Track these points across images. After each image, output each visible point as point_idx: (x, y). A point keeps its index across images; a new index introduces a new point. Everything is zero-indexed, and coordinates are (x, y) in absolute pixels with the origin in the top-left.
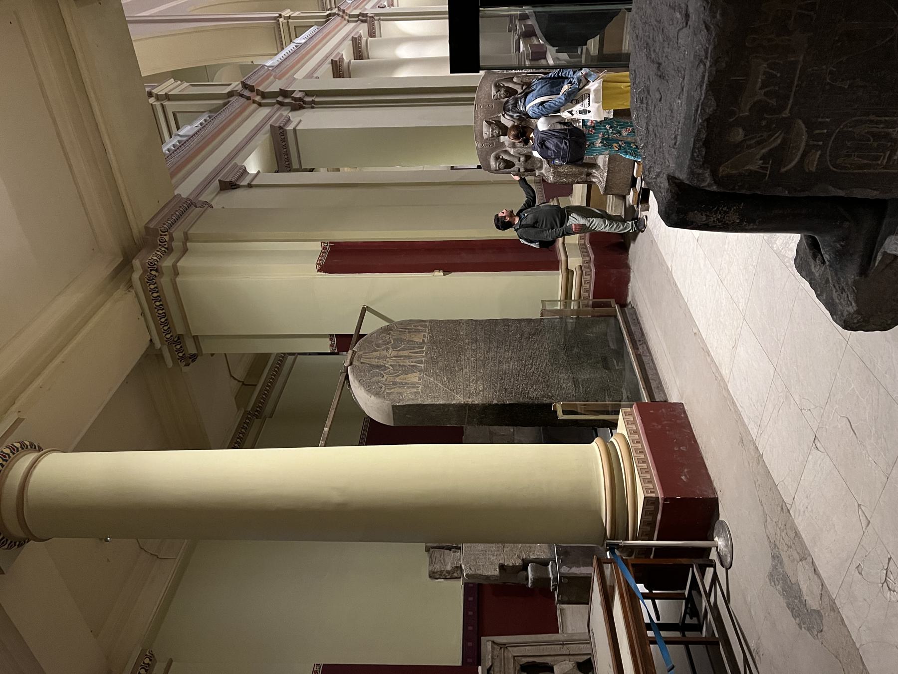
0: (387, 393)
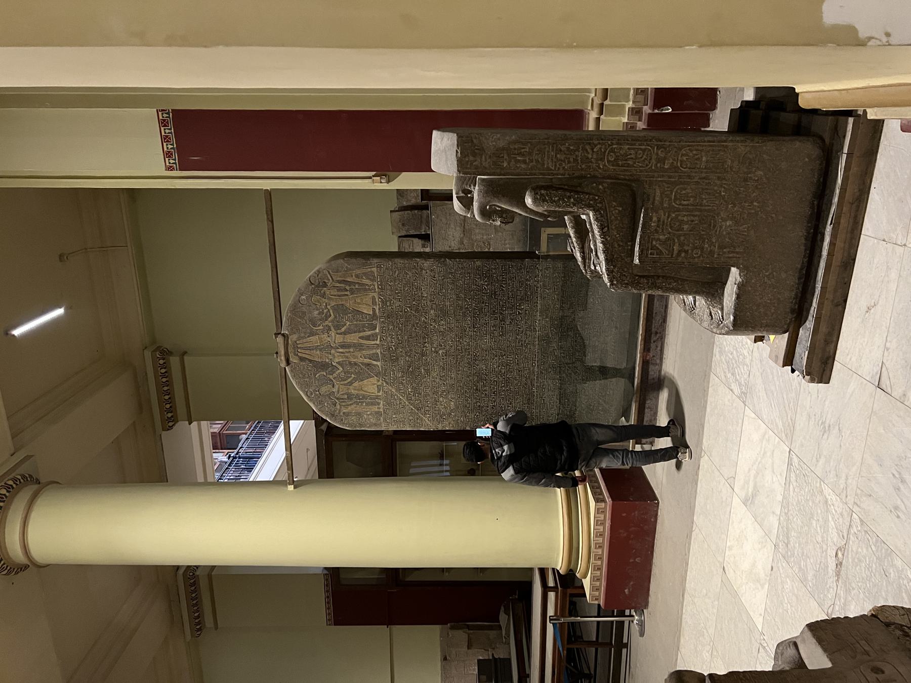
0: (344, 413)
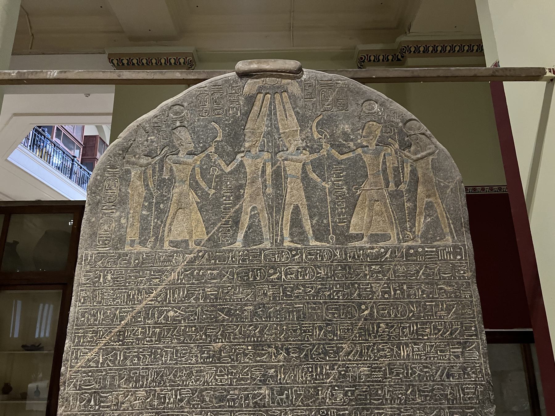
0: (128, 172)
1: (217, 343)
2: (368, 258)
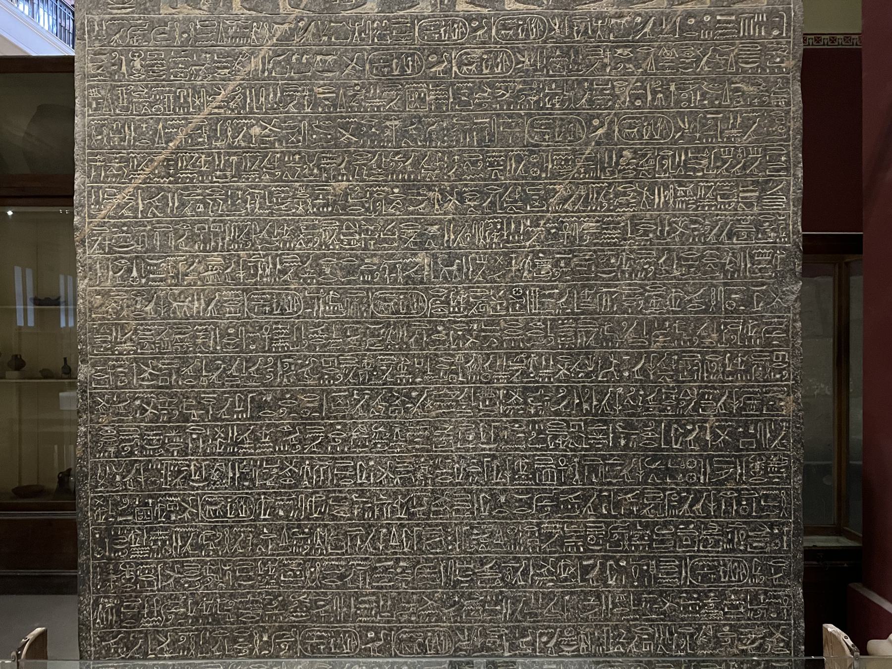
1: (339, 181)
2: (611, 35)
